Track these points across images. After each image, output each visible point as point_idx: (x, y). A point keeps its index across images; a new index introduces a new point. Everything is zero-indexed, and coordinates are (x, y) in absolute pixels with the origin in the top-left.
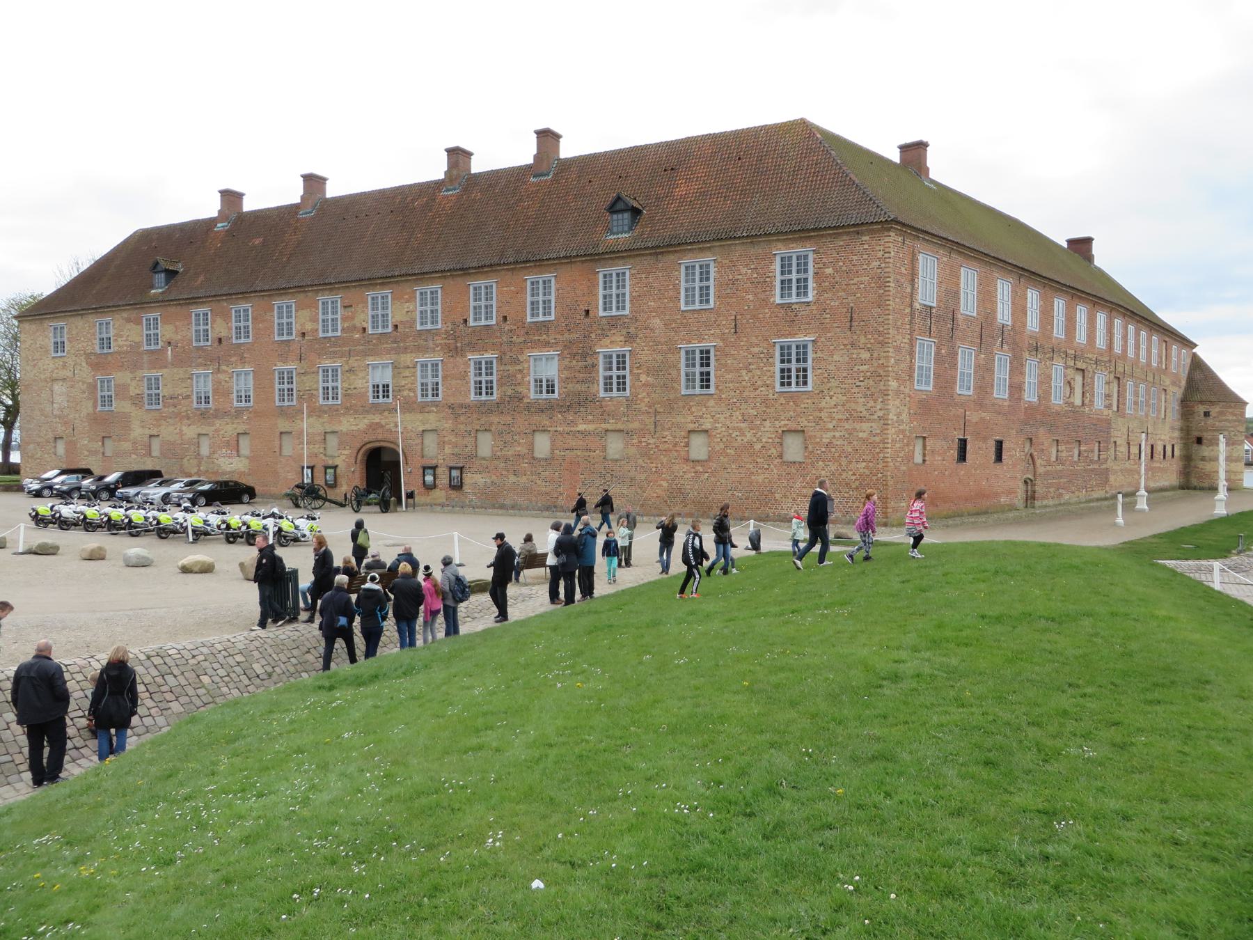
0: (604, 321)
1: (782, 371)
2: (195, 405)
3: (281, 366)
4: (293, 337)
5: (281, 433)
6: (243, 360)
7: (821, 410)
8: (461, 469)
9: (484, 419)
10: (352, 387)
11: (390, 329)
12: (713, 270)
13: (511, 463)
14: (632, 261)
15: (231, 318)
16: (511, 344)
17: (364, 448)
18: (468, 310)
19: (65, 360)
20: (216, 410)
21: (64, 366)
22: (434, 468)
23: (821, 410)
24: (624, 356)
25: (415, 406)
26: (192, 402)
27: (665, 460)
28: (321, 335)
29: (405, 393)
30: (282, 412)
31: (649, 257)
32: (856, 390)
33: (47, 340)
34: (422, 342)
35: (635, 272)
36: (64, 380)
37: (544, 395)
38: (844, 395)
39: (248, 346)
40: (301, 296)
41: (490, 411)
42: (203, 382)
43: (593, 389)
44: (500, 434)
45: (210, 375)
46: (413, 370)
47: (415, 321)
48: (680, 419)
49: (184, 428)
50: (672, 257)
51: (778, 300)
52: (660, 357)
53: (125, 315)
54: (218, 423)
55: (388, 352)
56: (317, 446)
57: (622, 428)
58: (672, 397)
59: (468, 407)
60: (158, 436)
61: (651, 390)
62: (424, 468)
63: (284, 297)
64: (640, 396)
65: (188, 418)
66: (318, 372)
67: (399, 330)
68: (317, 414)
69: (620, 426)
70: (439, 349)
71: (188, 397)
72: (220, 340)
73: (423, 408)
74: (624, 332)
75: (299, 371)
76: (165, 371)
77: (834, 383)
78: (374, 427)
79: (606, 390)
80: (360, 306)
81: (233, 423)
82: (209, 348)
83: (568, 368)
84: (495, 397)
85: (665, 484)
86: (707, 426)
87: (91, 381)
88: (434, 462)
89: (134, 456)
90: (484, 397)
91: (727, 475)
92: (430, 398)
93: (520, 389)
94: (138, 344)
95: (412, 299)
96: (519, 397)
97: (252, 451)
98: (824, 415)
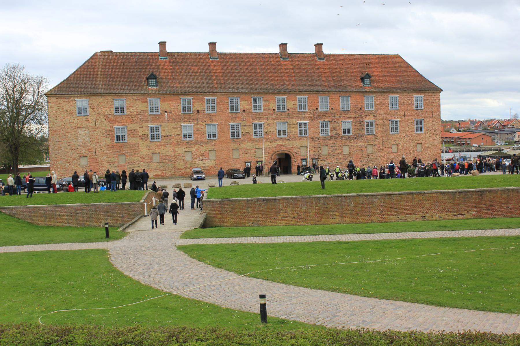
0: (366, 111)
1: (416, 127)
2: (183, 139)
3: (232, 123)
4: (239, 111)
5: (233, 149)
6: (211, 119)
7: (426, 138)
8: (317, 159)
9: (325, 142)
10: (269, 131)
11: (286, 110)
12: (398, 99)
14: (375, 94)
15: (204, 102)
16: (335, 117)
18: (318, 105)
19: (88, 117)
20: (196, 141)
21: (88, 120)
22: (306, 159)
23: (426, 138)
24: (373, 122)
26: (181, 137)
27: (385, 153)
28: (253, 111)
29: (293, 133)
30: (233, 141)
32: (434, 133)
33: (73, 107)
36: (87, 127)
37: (347, 134)
39: (214, 114)
40: (243, 96)
42: (188, 129)
43: (363, 132)
45: (192, 126)
46: (296, 125)
47: (297, 108)
49: (176, 149)
51: (415, 109)
53: (135, 97)
54: (197, 146)
55: (285, 118)
56: (252, 154)
57: (372, 144)
58: (387, 134)
59: (319, 138)
60: (159, 153)
62: (302, 160)
65: (179, 145)
66: (252, 125)
67: (290, 111)
68: (252, 141)
71: (178, 135)
73: (301, 139)
74: (373, 115)
76: (163, 124)
77: (429, 131)
78: (278, 145)
79: (367, 132)
81: (206, 146)
82: (191, 114)
84: (329, 134)
85: (386, 160)
87: (109, 128)
88: (306, 157)
89: (142, 163)
90: (325, 135)
92: (303, 135)
93: (338, 132)
94: (144, 112)
95: (295, 100)
96: (338, 135)
98: (427, 139)
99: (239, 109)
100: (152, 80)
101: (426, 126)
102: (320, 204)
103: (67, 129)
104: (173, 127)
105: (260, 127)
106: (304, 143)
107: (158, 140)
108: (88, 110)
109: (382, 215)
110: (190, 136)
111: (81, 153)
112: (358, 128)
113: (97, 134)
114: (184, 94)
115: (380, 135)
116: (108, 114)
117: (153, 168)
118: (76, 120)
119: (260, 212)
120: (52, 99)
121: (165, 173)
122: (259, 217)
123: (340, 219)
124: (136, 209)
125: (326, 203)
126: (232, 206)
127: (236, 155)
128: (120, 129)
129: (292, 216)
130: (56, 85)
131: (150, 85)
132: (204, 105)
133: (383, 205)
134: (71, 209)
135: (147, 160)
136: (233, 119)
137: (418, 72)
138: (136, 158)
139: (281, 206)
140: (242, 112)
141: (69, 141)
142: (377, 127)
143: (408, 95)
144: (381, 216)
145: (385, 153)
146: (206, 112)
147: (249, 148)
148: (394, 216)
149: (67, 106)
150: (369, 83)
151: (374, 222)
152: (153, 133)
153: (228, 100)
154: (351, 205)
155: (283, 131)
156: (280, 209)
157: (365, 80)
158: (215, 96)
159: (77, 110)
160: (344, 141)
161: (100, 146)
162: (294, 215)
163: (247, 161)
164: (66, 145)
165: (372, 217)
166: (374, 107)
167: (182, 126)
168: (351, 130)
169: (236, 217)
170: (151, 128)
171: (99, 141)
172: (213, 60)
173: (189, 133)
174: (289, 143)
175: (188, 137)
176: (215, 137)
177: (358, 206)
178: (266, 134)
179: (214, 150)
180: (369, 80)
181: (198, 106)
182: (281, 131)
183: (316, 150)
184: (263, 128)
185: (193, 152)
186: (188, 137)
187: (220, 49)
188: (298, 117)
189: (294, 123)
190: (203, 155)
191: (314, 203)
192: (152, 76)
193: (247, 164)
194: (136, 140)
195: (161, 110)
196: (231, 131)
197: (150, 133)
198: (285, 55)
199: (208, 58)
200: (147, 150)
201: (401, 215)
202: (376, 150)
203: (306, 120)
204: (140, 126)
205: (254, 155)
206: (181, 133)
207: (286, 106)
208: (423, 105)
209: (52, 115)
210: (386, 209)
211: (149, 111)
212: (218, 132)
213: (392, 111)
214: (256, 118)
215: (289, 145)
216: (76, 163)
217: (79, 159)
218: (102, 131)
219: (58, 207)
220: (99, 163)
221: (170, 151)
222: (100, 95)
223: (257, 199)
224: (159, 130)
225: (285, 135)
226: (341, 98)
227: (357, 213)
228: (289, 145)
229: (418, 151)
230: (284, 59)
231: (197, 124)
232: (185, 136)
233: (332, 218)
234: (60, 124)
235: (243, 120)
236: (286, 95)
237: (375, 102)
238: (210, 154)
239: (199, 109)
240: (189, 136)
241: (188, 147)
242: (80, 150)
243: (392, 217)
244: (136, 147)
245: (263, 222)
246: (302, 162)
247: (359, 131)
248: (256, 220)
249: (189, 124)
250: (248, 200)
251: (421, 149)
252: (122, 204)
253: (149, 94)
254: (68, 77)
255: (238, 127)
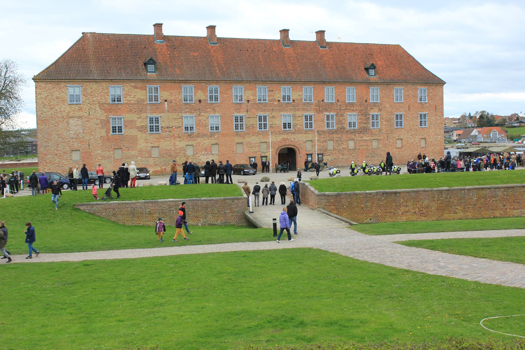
2: (184, 131)
3: (236, 114)
4: (243, 102)
5: (237, 143)
6: (214, 110)
7: (429, 132)
8: (322, 154)
9: (331, 136)
10: (274, 124)
11: (291, 101)
12: (403, 91)
13: (341, 151)
14: (380, 86)
15: (207, 91)
16: (340, 110)
17: (280, 148)
18: (324, 97)
19: (81, 106)
20: (198, 133)
21: (80, 109)
22: (311, 155)
23: (429, 132)
25: (303, 131)
26: (182, 130)
27: (390, 148)
28: (258, 102)
29: (298, 126)
30: (237, 134)
31: (385, 85)
33: (64, 94)
34: (305, 107)
35: (381, 89)
36: (80, 117)
37: (352, 128)
38: (434, 128)
39: (217, 104)
40: (247, 84)
41: (333, 133)
42: (189, 120)
43: (369, 126)
44: (337, 141)
45: (194, 117)
46: (302, 118)
47: (302, 99)
48: (394, 135)
49: (176, 142)
50: (391, 86)
52: (389, 116)
53: (133, 84)
54: (199, 140)
55: (291, 110)
56: (256, 148)
58: (392, 128)
60: (159, 147)
61: (386, 126)
62: (308, 155)
63: (238, 84)
64: (383, 128)
65: (180, 137)
67: (295, 102)
68: (256, 135)
69: (377, 138)
70: (313, 110)
71: (179, 127)
72: (200, 101)
73: (306, 132)
75: (246, 117)
76: (163, 115)
77: (432, 125)
78: (284, 140)
79: (372, 126)
80: (277, 91)
81: (209, 139)
82: (193, 104)
83: (360, 119)
86: (402, 137)
87: (104, 118)
88: (311, 153)
89: (140, 158)
90: (330, 128)
91: (407, 152)
93: (344, 125)
94: (143, 100)
96: (344, 128)
97: (219, 151)
99: (243, 99)
100: (151, 66)
101: (429, 120)
102: (442, 197)
103: (57, 119)
104: (173, 118)
105: (265, 120)
106: (310, 137)
107: (157, 132)
108: (81, 97)
109: (505, 209)
110: (192, 128)
111: (73, 146)
112: (363, 121)
113: (91, 125)
114: (186, 81)
115: (385, 130)
116: (103, 102)
117: (152, 163)
118: (68, 109)
119: (379, 206)
120: (40, 84)
121: (165, 169)
122: (378, 213)
123: (462, 214)
124: (240, 205)
125: (448, 197)
126: (349, 200)
127: (239, 149)
128: (117, 119)
129: (413, 211)
130: (44, 69)
131: (149, 70)
132: (206, 94)
133: (506, 199)
134: (164, 206)
135: (145, 155)
136: (238, 110)
137: (420, 64)
138: (133, 153)
139: (402, 200)
140: (247, 103)
141: (60, 133)
142: (382, 120)
143: (412, 87)
144: (504, 210)
145: (390, 148)
146: (209, 102)
147: (253, 142)
148: (517, 211)
149: (57, 93)
150: (374, 74)
151: (497, 217)
152: (152, 125)
153: (232, 90)
154: (474, 198)
155: (288, 123)
156: (400, 204)
157: (370, 70)
158: (219, 85)
159: (68, 97)
160: (349, 136)
161: (94, 138)
162: (415, 210)
163: (251, 156)
164: (56, 137)
165: (494, 211)
166: (379, 99)
167: (184, 117)
168: (356, 123)
169: (354, 213)
170: (150, 118)
171: (93, 133)
172: (212, 45)
173: (190, 125)
174: (294, 137)
175: (189, 129)
176: (218, 129)
177: (481, 200)
178: (271, 127)
179: (217, 144)
180: (374, 70)
181: (201, 95)
182: (286, 124)
183: (322, 144)
184: (267, 120)
185: (195, 145)
186: (189, 129)
187: (220, 33)
188: (304, 109)
189: (300, 115)
190: (206, 149)
191: (436, 196)
192: (152, 62)
193: (251, 159)
194: (134, 132)
195: (161, 99)
196: (234, 123)
197: (149, 125)
198: (287, 42)
199: (207, 43)
200: (146, 144)
201: (524, 209)
202: (380, 146)
203: (311, 112)
204: (138, 116)
205: (259, 150)
206: (183, 124)
207: (291, 97)
208: (427, 98)
209: (41, 102)
210: (509, 203)
211: (148, 100)
212: (221, 124)
213: (396, 104)
214: (261, 110)
215: (294, 139)
216: (68, 157)
217: (71, 153)
218: (96, 122)
219: (148, 203)
220: (93, 158)
221: (171, 144)
222: (95, 81)
223: (377, 192)
224: (158, 121)
225: (290, 128)
226: (346, 89)
227: (479, 207)
228: (294, 139)
229: (422, 146)
230: (286, 46)
231: (199, 115)
232: (187, 128)
233: (454, 213)
234: (50, 113)
235: (247, 112)
236: (291, 84)
237: (380, 94)
238: (212, 148)
239: (201, 99)
240: (190, 128)
241: (190, 140)
242: (72, 143)
243: (515, 211)
244: (134, 140)
245: (382, 217)
246: (307, 158)
247: (364, 125)
248: (375, 216)
249: (191, 114)
250: (366, 193)
251: (425, 144)
252: (224, 200)
253: (148, 81)
254: (57, 61)
255: (242, 119)
